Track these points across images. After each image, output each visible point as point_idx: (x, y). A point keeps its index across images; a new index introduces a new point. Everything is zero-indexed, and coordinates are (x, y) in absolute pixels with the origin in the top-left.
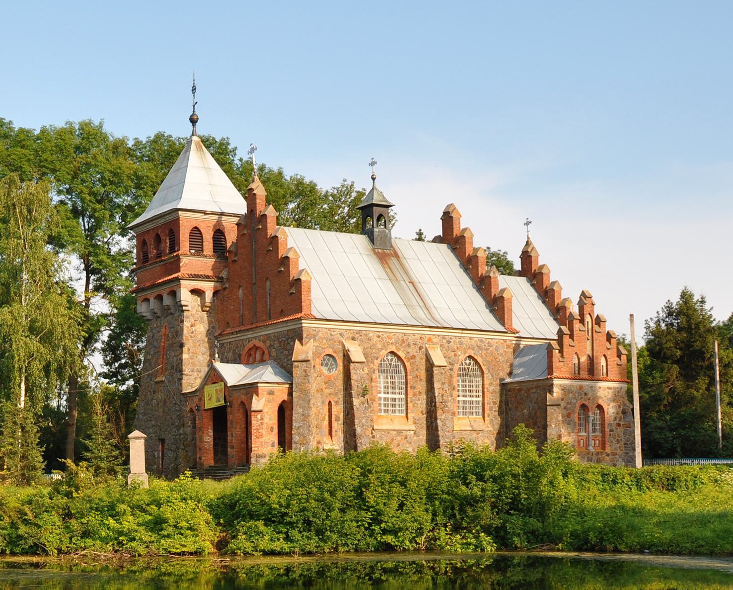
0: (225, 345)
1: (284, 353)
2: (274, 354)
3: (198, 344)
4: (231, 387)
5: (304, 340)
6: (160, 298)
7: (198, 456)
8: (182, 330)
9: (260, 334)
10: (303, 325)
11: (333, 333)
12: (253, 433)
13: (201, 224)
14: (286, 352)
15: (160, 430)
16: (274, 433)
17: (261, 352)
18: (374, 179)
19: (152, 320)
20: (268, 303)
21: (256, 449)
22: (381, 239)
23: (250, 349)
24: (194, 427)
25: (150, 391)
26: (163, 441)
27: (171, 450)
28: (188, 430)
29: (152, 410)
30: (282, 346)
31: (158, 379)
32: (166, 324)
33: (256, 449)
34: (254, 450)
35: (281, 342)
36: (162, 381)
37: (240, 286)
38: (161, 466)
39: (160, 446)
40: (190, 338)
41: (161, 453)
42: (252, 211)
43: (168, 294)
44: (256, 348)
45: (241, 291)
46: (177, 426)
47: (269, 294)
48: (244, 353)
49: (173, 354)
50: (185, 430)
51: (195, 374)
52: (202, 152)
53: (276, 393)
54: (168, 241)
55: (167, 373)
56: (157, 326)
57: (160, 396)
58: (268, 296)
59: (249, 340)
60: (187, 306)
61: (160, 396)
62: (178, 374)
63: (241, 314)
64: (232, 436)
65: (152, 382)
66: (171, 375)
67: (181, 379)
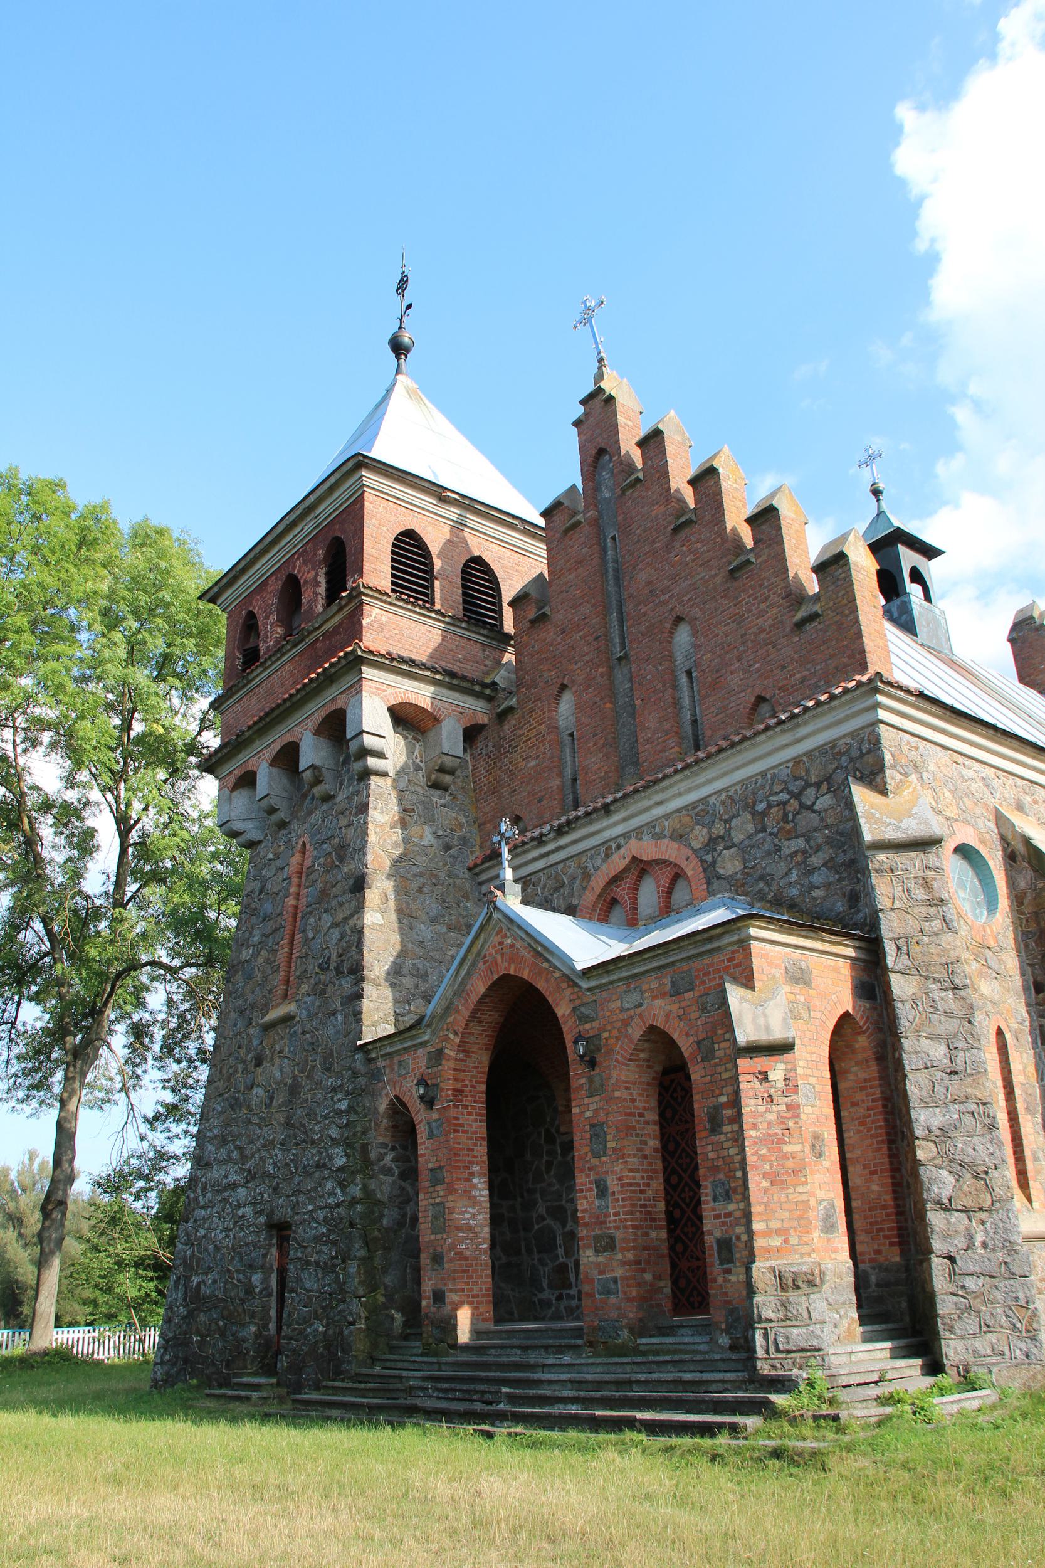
1: (786, 851)
2: (730, 864)
3: (414, 886)
4: (588, 972)
5: (891, 776)
6: (288, 757)
7: (427, 1287)
8: (365, 833)
9: (658, 811)
10: (882, 714)
11: (965, 772)
12: (751, 1159)
13: (429, 529)
14: (800, 843)
15: (275, 1189)
16: (826, 1164)
17: (665, 881)
18: (876, 493)
19: (260, 842)
20: (686, 702)
21: (776, 1242)
22: (928, 625)
23: (616, 879)
24: (409, 1172)
25: (244, 1062)
26: (281, 1230)
28: (384, 1186)
29: (249, 1122)
32: (307, 838)
33: (776, 1242)
34: (768, 1250)
35: (764, 814)
36: (288, 1019)
37: (563, 687)
38: (272, 1326)
39: (274, 1251)
41: (274, 1278)
42: (601, 452)
43: (317, 733)
44: (641, 868)
46: (341, 1169)
47: (689, 673)
48: (589, 897)
49: (327, 920)
50: (373, 1185)
52: (423, 407)
53: (817, 981)
54: (322, 580)
55: (305, 988)
56: (277, 856)
57: (276, 1071)
58: (684, 680)
59: (607, 849)
60: (380, 755)
61: (276, 1071)
62: (346, 983)
63: (568, 772)
65: (252, 1031)
66: (319, 991)
67: (360, 996)
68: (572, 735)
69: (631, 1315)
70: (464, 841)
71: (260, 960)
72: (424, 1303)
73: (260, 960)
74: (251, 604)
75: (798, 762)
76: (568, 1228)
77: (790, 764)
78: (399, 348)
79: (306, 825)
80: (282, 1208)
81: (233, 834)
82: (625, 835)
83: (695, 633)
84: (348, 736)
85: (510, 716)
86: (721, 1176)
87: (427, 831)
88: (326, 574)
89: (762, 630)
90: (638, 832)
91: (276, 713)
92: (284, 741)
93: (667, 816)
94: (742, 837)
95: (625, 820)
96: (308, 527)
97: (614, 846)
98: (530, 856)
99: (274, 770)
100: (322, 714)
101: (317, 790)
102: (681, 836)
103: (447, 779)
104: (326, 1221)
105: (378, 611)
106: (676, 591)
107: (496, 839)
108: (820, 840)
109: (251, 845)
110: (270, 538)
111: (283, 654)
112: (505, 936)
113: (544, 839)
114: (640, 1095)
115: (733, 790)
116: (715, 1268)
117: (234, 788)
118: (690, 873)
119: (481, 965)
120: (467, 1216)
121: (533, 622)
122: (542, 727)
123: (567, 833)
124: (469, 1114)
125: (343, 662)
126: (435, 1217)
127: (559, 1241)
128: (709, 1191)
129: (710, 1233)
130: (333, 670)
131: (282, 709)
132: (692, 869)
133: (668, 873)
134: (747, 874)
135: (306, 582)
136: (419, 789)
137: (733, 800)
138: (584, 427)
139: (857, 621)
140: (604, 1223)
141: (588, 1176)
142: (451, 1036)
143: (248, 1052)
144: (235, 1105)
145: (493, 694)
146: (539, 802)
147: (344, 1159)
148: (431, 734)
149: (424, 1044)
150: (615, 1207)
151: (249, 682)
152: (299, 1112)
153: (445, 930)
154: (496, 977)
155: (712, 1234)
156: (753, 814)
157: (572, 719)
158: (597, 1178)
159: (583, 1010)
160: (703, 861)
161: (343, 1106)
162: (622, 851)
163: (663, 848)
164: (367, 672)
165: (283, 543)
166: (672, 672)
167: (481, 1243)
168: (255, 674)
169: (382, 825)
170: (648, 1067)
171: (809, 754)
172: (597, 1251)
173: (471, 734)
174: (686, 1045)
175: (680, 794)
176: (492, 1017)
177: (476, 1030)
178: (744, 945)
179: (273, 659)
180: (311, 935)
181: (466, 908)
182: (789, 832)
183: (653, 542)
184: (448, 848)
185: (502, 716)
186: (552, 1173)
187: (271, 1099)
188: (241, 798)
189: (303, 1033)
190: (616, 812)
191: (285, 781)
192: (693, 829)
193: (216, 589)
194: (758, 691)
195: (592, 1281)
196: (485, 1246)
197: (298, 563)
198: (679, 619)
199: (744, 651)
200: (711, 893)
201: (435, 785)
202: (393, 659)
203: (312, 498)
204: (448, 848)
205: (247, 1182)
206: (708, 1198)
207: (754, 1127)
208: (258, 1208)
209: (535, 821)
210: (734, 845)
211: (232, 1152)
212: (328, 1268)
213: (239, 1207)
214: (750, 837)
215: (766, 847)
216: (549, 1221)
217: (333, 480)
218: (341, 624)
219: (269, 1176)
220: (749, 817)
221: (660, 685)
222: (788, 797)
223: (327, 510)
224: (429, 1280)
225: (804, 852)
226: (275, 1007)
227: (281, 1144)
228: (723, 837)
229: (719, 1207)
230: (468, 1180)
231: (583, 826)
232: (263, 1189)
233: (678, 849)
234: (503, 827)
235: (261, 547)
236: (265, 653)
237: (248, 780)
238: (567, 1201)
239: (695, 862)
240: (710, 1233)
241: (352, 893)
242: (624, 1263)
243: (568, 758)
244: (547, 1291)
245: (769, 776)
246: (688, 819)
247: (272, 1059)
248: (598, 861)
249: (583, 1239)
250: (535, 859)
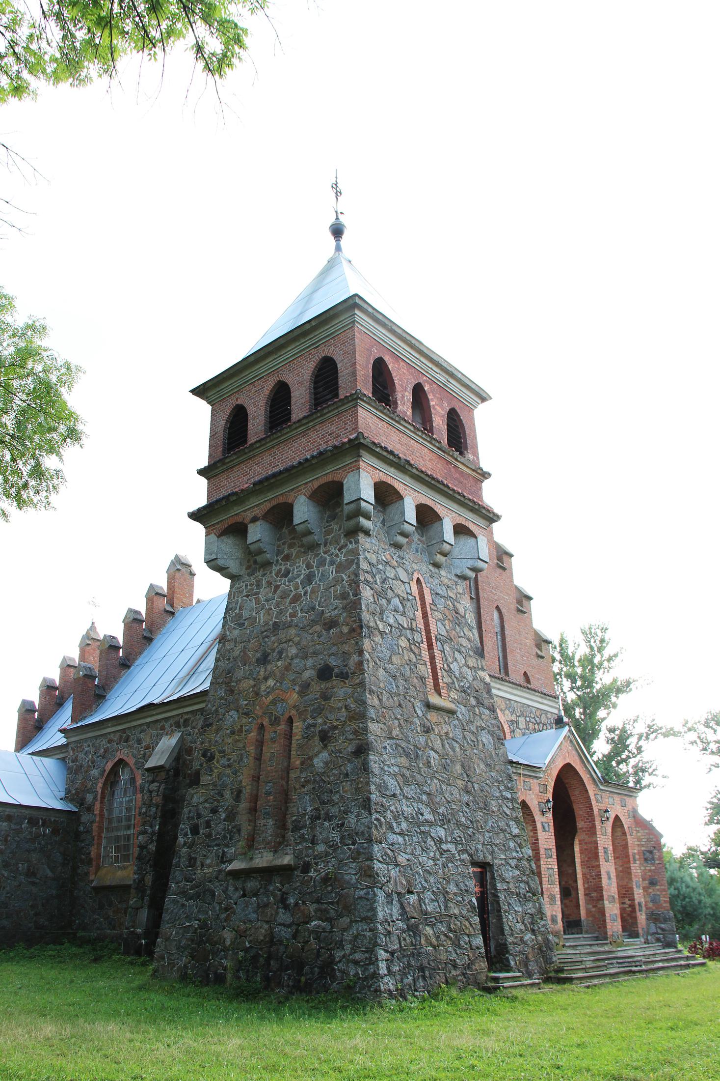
36: (452, 712)
46: (517, 836)
78: (337, 232)
96: (442, 377)
101: (440, 558)
104: (517, 867)
111: (430, 442)
116: (638, 913)
131: (446, 489)
149: (537, 778)
152: (476, 786)
161: (509, 796)
165: (422, 359)
193: (370, 310)
203: (460, 376)
217: (473, 386)
223: (454, 386)
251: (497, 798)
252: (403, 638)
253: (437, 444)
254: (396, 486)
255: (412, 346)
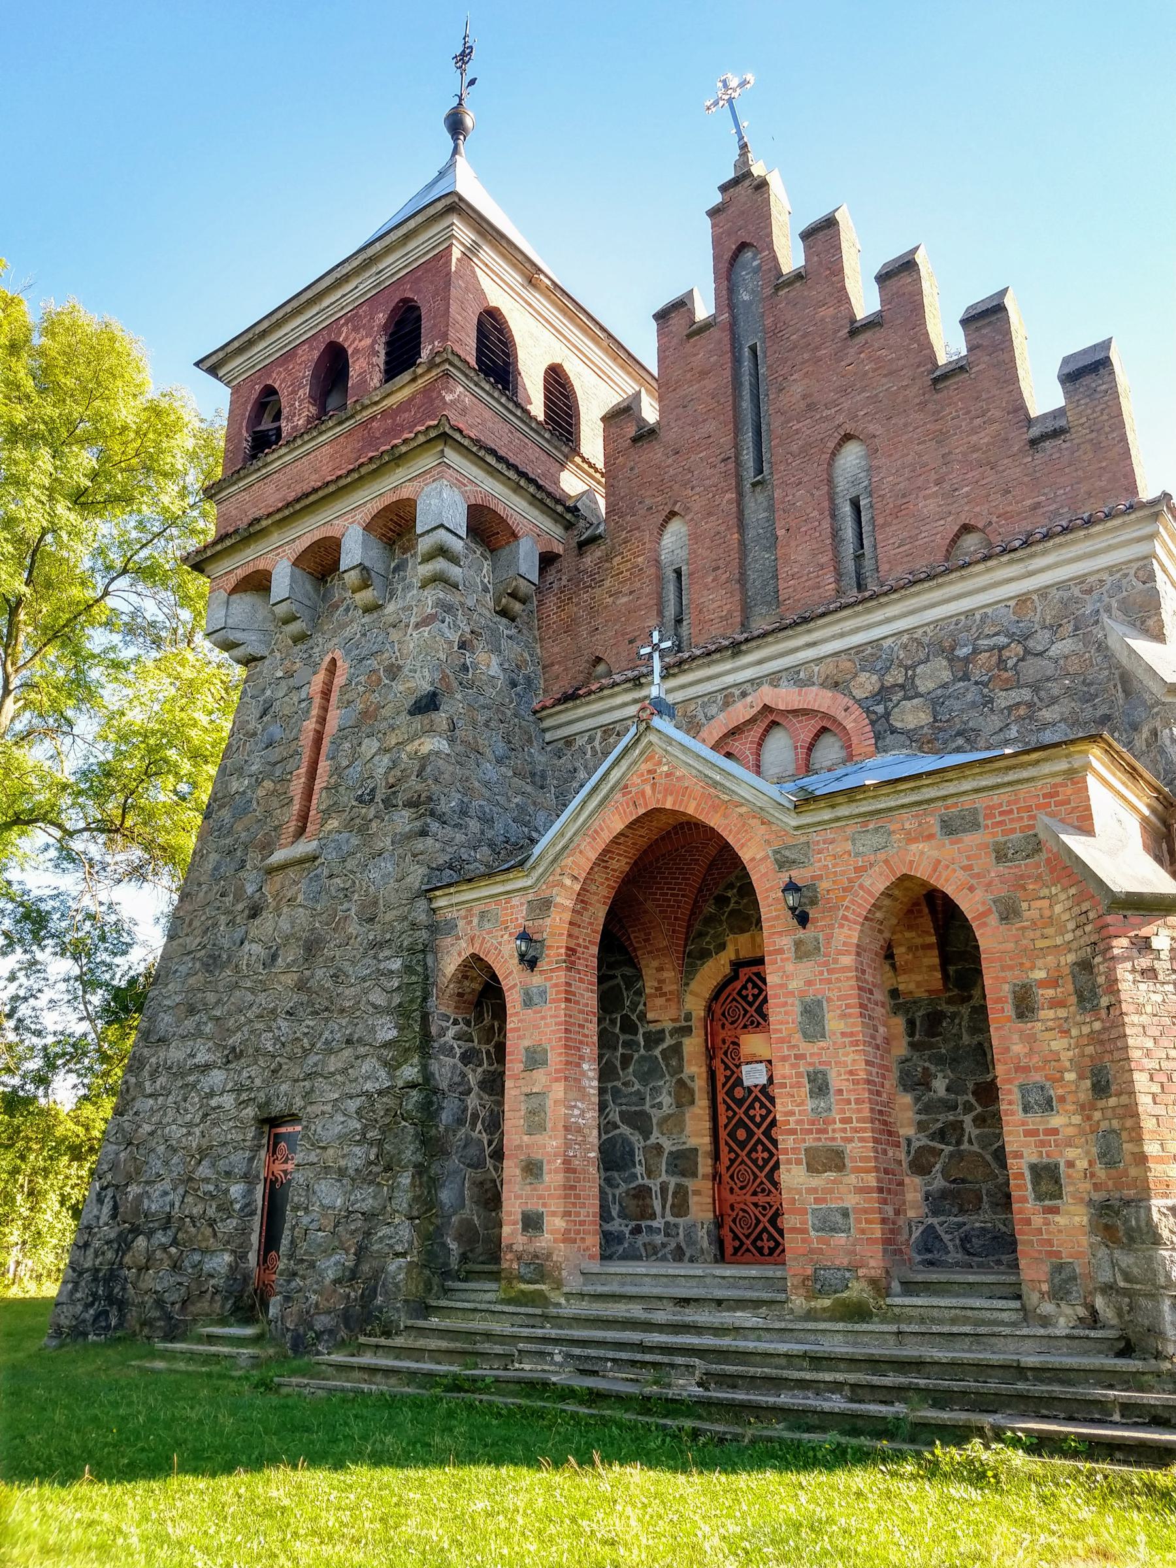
0: (581, 741)
2: (912, 715)
3: (481, 719)
7: (513, 1206)
14: (1026, 694)
17: (806, 736)
19: (263, 658)
23: (735, 732)
25: (228, 912)
27: (342, 1172)
30: (977, 674)
31: (279, 856)
32: (338, 654)
35: (967, 660)
39: (263, 1153)
40: (455, 684)
42: (743, 246)
45: (674, 540)
46: (387, 1045)
49: (370, 746)
51: (474, 825)
55: (333, 824)
56: (289, 675)
58: (847, 509)
60: (454, 559)
64: (819, 1086)
68: (678, 572)
69: (872, 1263)
70: (529, 680)
71: (261, 792)
72: (506, 1230)
73: (261, 792)
74: (270, 376)
75: (1025, 601)
76: (652, 1140)
77: (1012, 603)
79: (335, 640)
80: (285, 1095)
81: (227, 646)
82: (755, 682)
83: (872, 452)
84: (419, 531)
85: (593, 547)
86: (1037, 1077)
87: (495, 660)
88: (387, 344)
89: (975, 448)
90: (774, 679)
91: (312, 498)
92: (317, 535)
93: (819, 660)
94: (931, 685)
95: (760, 662)
97: (737, 693)
98: (618, 700)
99: (297, 571)
100: (379, 505)
102: (836, 684)
103: (517, 607)
105: (460, 389)
106: (846, 405)
107: (648, 650)
108: (1055, 692)
109: (248, 661)
110: (309, 294)
111: (321, 434)
112: (660, 763)
113: (643, 680)
114: (870, 966)
115: (920, 631)
117: (234, 591)
118: (849, 726)
119: (618, 796)
120: (576, 1112)
121: (635, 440)
122: (640, 559)
123: (674, 675)
124: (581, 980)
125: (422, 439)
126: (532, 1112)
127: (639, 1156)
128: (1016, 1096)
129: (1018, 1155)
130: (404, 449)
132: (854, 721)
133: (814, 725)
134: (940, 729)
135: (356, 351)
136: (487, 613)
137: (920, 643)
138: (723, 216)
139: (1124, 439)
140: (825, 1131)
141: (793, 1066)
142: (568, 882)
143: (237, 900)
144: (213, 962)
145: (573, 520)
146: (631, 642)
147: (395, 1033)
148: (504, 553)
150: (843, 1111)
151: (265, 466)
152: (320, 973)
153: (510, 773)
154: (641, 811)
155: (1021, 1157)
156: (950, 660)
157: (684, 554)
158: (811, 1069)
159: (787, 853)
160: (868, 711)
162: (749, 699)
163: (811, 697)
164: (453, 457)
165: (326, 302)
166: (832, 497)
167: (589, 1150)
168: (275, 455)
169: (451, 643)
170: (880, 931)
171: (1043, 592)
172: (811, 1169)
173: (547, 560)
174: (968, 905)
175: (842, 635)
176: (621, 864)
177: (599, 877)
178: (1076, 777)
179: (306, 438)
180: (345, 763)
181: (531, 755)
182: (1007, 679)
183: (817, 348)
184: (514, 684)
185: (583, 546)
186: (631, 1069)
187: (274, 957)
188: (244, 604)
189: (331, 876)
190: (746, 652)
191: (309, 587)
192: (856, 675)
194: (964, 519)
195: (804, 1212)
196: (592, 1155)
197: (345, 329)
198: (848, 437)
199: (947, 474)
200: (880, 749)
201: (503, 613)
202: (481, 447)
204: (514, 684)
205: (228, 1062)
206: (1014, 1107)
207: (1140, 1009)
208: (244, 1096)
209: (624, 664)
210: (918, 695)
211: (205, 1024)
212: (364, 1177)
213: (211, 1095)
214: (944, 686)
215: (969, 697)
216: (625, 1130)
218: (411, 399)
219: (267, 1054)
220: (945, 663)
221: (815, 513)
222: (1006, 640)
223: (393, 265)
224: (516, 1197)
225: (1030, 705)
226: (282, 846)
227: (288, 1012)
228: (902, 687)
229: (1034, 1121)
230: (579, 1065)
231: (699, 667)
232: (253, 1073)
233: (834, 699)
234: (656, 637)
235: (295, 304)
236: (289, 434)
237: (258, 583)
238: (653, 1106)
239: (857, 712)
240: (1018, 1155)
241: (411, 713)
242: (860, 1190)
243: (672, 596)
244: (618, 1221)
245: (978, 617)
246: (849, 664)
247: (277, 909)
248: (713, 710)
249: (786, 1152)
250: (625, 705)
251: (364, 980)
252: (265, 783)
253: (330, 424)
254: (261, 565)
255: (298, 311)
